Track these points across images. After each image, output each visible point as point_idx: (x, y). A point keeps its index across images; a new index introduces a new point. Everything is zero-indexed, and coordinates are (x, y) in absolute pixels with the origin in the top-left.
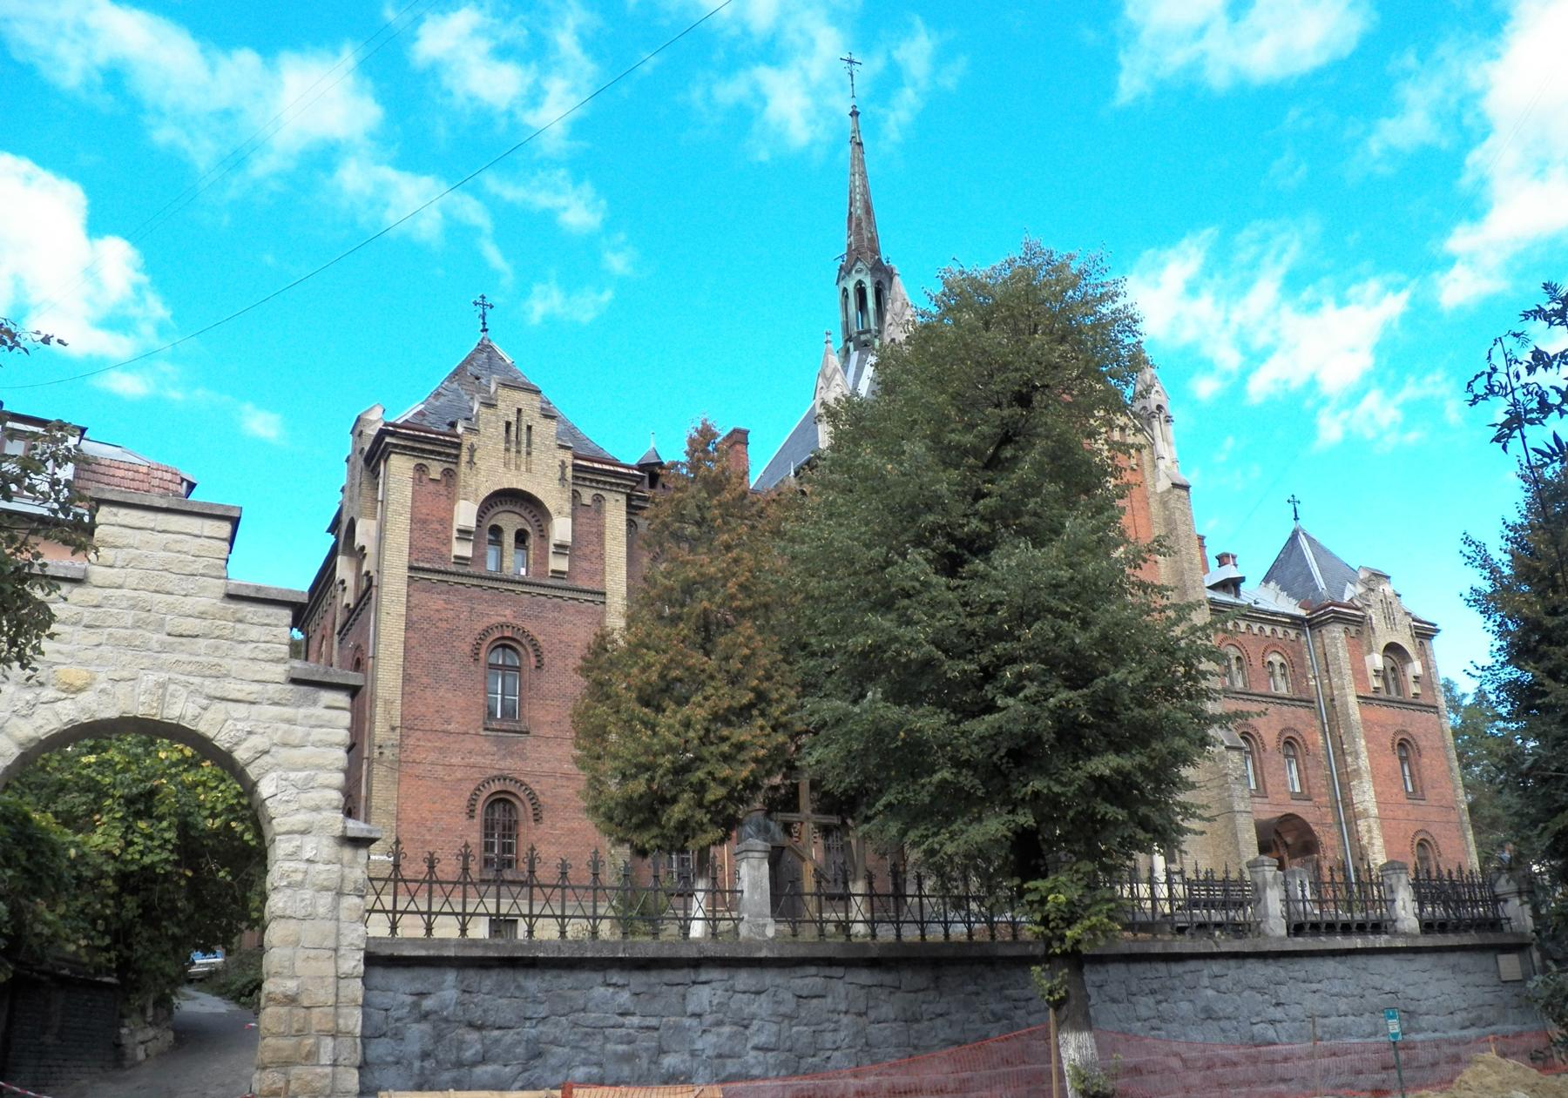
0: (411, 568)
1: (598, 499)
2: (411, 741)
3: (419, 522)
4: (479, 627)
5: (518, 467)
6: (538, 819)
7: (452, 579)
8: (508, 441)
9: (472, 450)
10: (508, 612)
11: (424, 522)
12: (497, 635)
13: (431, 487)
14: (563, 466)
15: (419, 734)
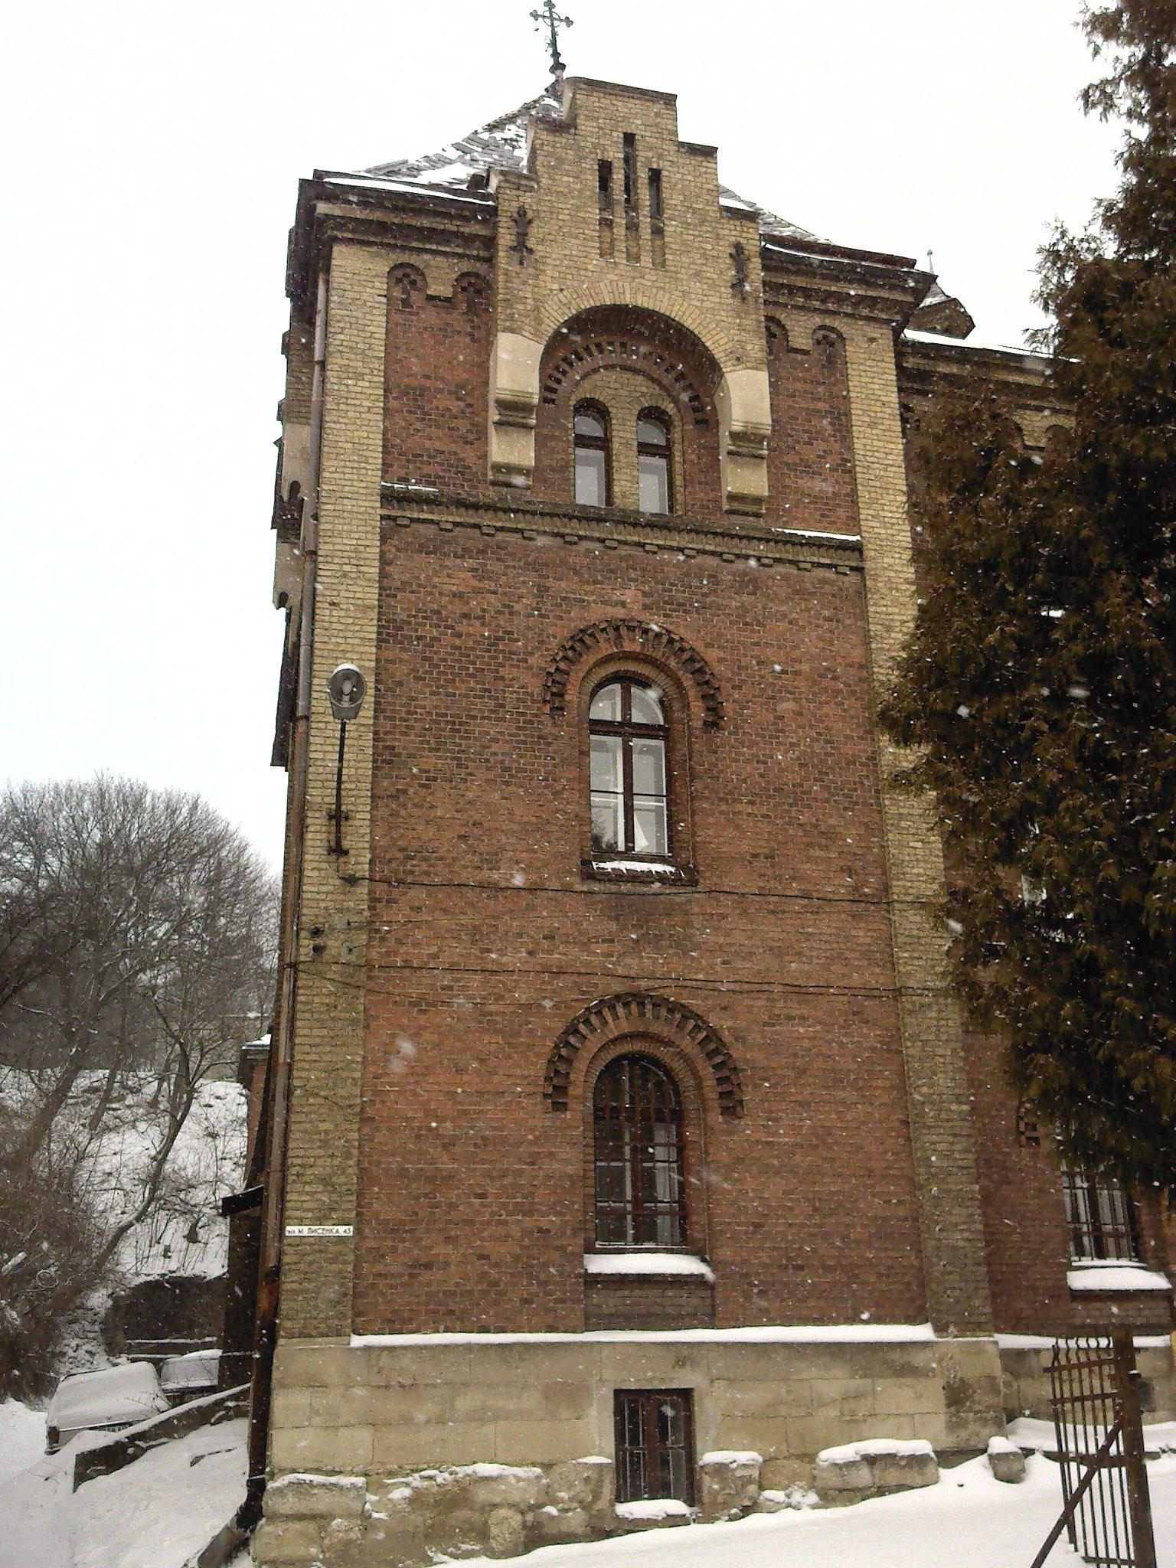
0: (388, 497)
1: (830, 343)
2: (400, 913)
3: (403, 395)
4: (559, 632)
5: (633, 257)
6: (732, 1107)
7: (487, 520)
8: (607, 203)
9: (522, 221)
10: (629, 596)
11: (423, 391)
12: (606, 649)
13: (431, 316)
14: (738, 255)
15: (418, 895)
